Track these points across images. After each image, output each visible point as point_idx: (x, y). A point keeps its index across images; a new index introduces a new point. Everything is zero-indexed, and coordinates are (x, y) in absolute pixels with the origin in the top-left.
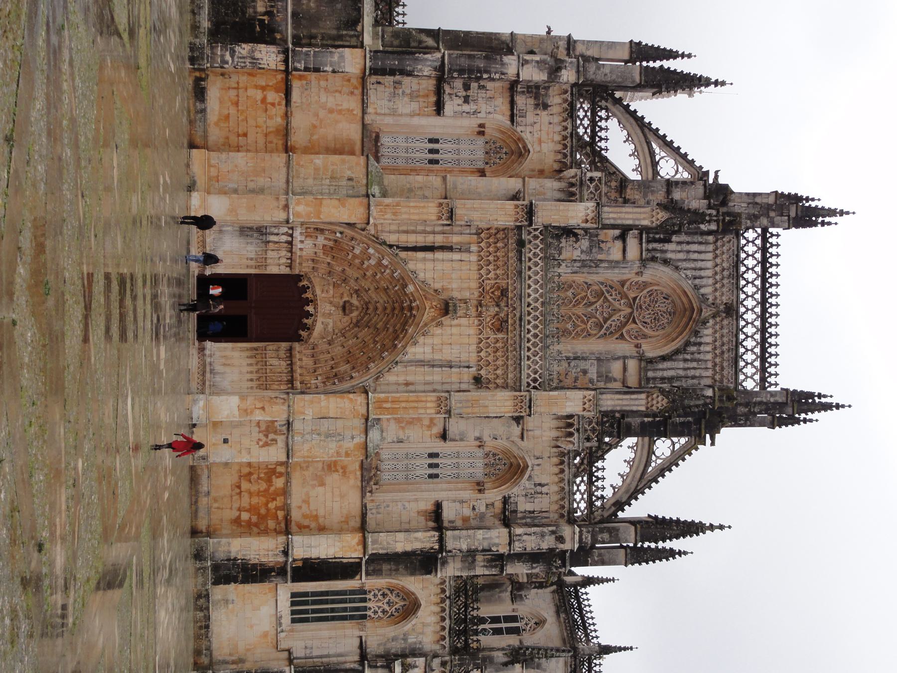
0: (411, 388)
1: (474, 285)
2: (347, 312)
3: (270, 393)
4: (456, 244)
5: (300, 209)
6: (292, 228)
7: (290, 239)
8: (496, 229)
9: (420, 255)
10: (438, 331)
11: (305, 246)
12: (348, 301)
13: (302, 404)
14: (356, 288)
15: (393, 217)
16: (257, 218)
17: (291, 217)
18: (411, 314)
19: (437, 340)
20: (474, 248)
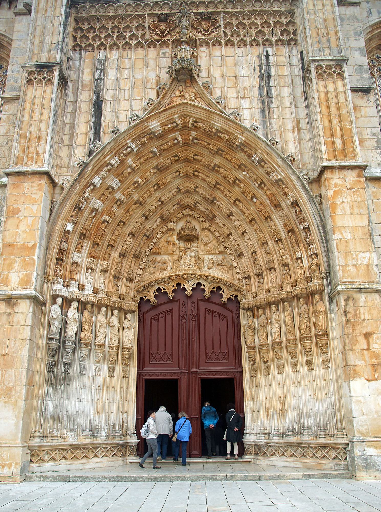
0: (304, 124)
1: (152, 53)
2: (193, 233)
3: (335, 331)
4: (94, 74)
6: (54, 298)
7: (74, 304)
8: (75, 30)
9: (107, 116)
10: (218, 93)
11: (90, 282)
12: (178, 234)
13: (353, 270)
14: (159, 220)
18: (196, 128)
19: (232, 93)
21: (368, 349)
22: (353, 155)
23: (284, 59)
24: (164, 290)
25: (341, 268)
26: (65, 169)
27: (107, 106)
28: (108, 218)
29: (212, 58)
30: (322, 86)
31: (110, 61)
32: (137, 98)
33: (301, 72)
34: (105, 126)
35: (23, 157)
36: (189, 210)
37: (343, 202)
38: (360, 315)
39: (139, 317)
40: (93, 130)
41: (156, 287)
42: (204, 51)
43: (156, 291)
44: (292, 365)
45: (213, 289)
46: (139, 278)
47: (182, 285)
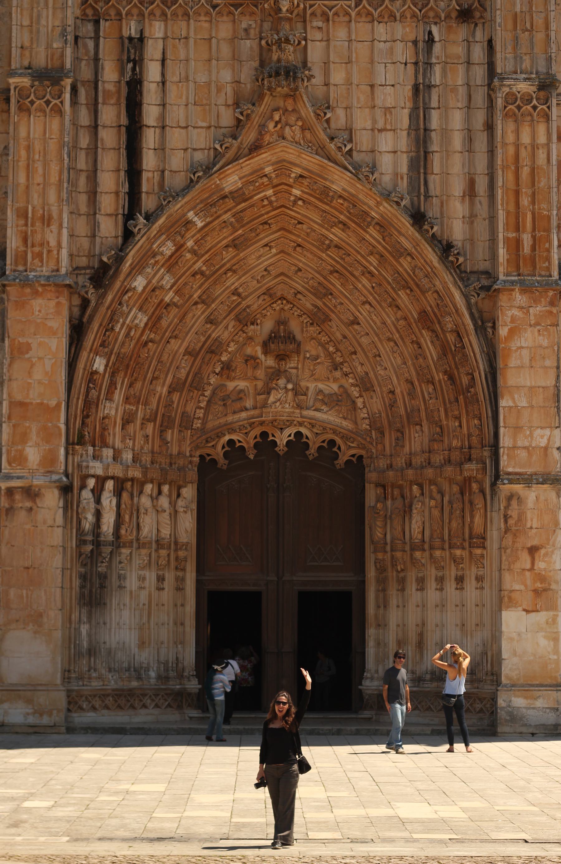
1: (224, 29)
4: (122, 72)
5: (33, 455)
9: (149, 161)
12: (265, 346)
13: (523, 454)
15: (54, 228)
16: (57, 561)
17: (55, 477)
20: (131, 29)
21: (532, 569)
22: (547, 264)
23: (459, 50)
24: (240, 444)
25: (506, 452)
26: (84, 258)
27: (150, 139)
28: (152, 336)
29: (332, 43)
30: (512, 132)
31: (150, 42)
32: (201, 124)
33: (486, 83)
34: (148, 179)
35: (26, 253)
36: (284, 302)
37: (522, 347)
38: (526, 520)
39: (198, 489)
40: (126, 188)
41: (227, 438)
42: (319, 28)
43: (226, 446)
44: (436, 579)
45: (322, 444)
46: (199, 425)
47: (270, 436)
